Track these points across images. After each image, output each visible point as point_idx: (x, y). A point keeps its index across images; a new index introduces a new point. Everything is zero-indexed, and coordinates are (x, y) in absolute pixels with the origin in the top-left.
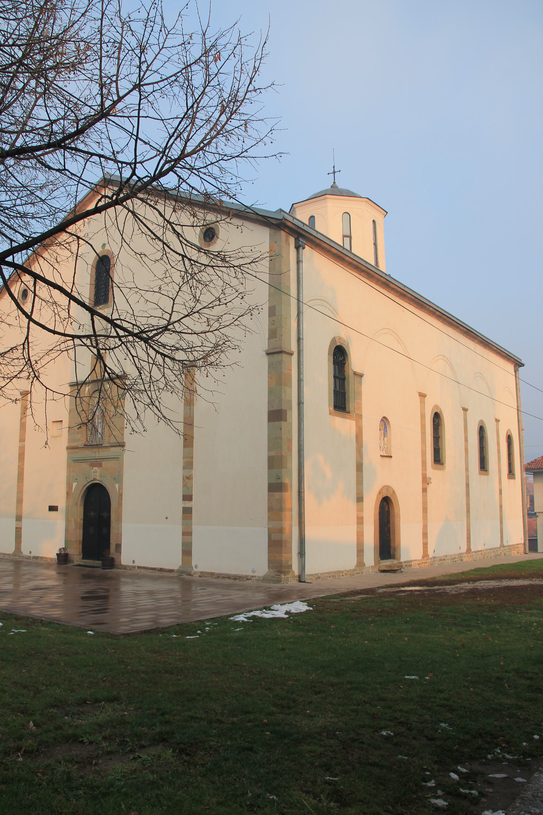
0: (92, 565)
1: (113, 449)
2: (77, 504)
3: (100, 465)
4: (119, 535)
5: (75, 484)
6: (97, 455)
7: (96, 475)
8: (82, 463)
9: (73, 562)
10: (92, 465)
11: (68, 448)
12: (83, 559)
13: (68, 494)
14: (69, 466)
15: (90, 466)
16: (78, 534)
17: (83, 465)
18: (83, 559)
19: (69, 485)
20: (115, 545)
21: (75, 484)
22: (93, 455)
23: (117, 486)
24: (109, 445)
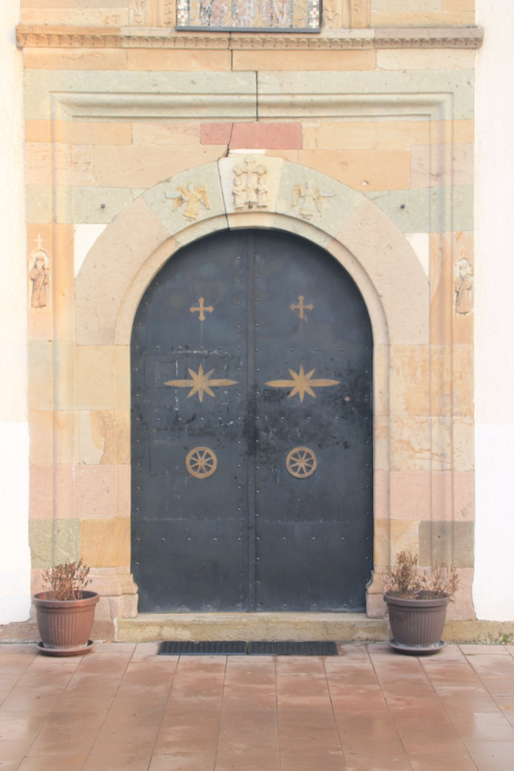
0: (259, 636)
1: (386, 58)
2: (109, 334)
3: (286, 140)
4: (452, 476)
5: (86, 237)
6: (271, 86)
7: (259, 187)
8: (137, 125)
9: (108, 630)
10: (225, 136)
11: (22, 37)
12: (142, 608)
13: (39, 282)
14: (38, 133)
15: (207, 136)
16: (108, 492)
17: (146, 133)
18: (142, 608)
19: (48, 238)
20: (415, 529)
21: (86, 237)
22: (243, 83)
23: (420, 244)
24: (369, 34)
